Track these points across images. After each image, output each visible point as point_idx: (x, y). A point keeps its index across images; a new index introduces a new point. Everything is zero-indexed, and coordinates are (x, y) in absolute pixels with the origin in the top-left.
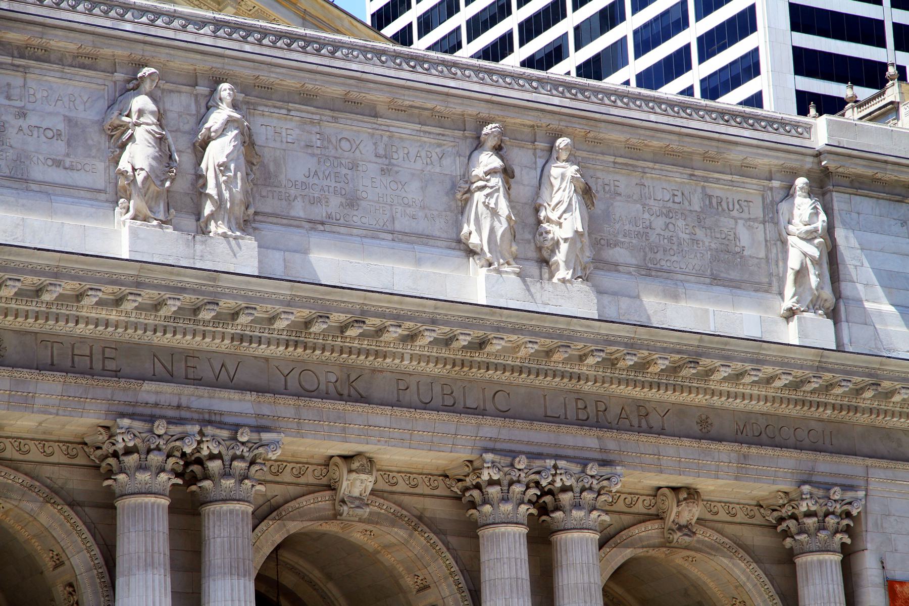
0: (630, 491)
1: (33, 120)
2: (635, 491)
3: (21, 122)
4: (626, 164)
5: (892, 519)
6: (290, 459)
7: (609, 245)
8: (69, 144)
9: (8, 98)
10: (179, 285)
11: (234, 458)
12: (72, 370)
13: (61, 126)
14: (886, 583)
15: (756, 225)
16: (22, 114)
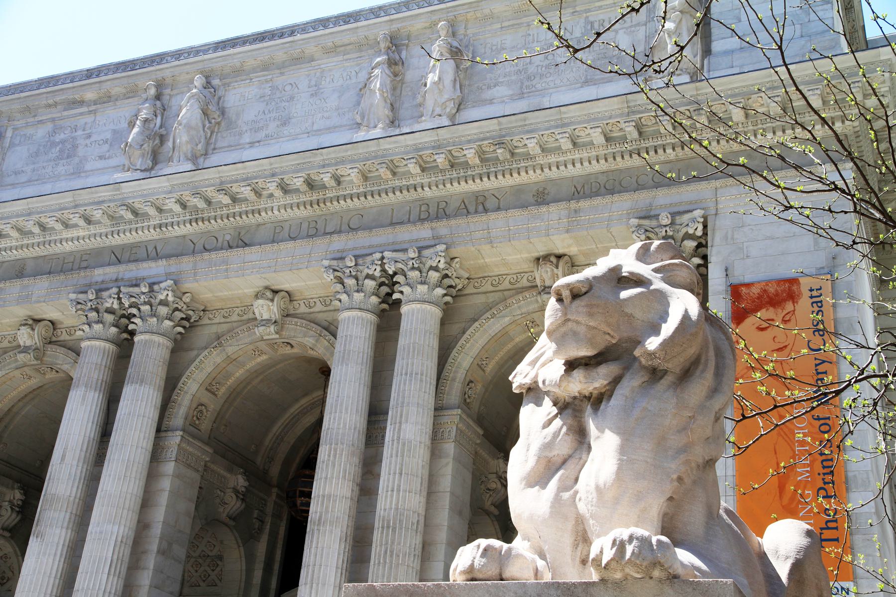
0: (516, 271)
1: (94, 137)
2: (522, 271)
3: (88, 142)
4: (513, 25)
5: (746, 229)
6: (239, 305)
7: (489, 87)
8: (111, 145)
9: (84, 130)
10: (101, 199)
11: (177, 309)
12: (62, 271)
13: (108, 135)
14: (729, 289)
15: (638, 28)
16: (89, 136)
